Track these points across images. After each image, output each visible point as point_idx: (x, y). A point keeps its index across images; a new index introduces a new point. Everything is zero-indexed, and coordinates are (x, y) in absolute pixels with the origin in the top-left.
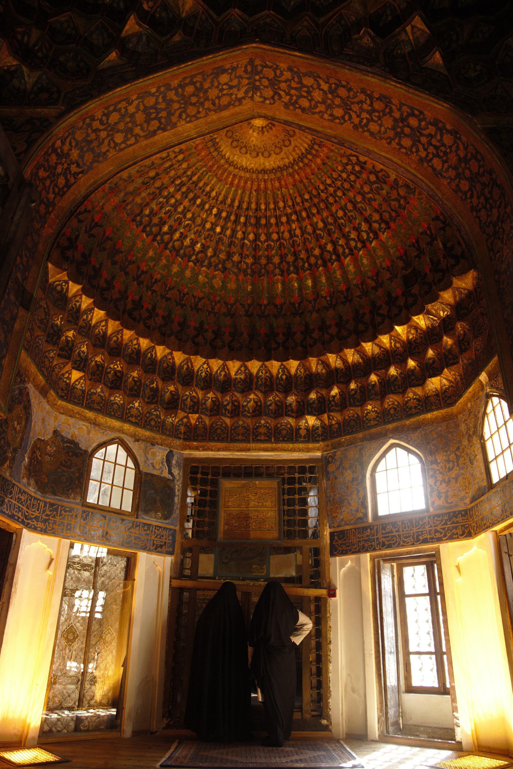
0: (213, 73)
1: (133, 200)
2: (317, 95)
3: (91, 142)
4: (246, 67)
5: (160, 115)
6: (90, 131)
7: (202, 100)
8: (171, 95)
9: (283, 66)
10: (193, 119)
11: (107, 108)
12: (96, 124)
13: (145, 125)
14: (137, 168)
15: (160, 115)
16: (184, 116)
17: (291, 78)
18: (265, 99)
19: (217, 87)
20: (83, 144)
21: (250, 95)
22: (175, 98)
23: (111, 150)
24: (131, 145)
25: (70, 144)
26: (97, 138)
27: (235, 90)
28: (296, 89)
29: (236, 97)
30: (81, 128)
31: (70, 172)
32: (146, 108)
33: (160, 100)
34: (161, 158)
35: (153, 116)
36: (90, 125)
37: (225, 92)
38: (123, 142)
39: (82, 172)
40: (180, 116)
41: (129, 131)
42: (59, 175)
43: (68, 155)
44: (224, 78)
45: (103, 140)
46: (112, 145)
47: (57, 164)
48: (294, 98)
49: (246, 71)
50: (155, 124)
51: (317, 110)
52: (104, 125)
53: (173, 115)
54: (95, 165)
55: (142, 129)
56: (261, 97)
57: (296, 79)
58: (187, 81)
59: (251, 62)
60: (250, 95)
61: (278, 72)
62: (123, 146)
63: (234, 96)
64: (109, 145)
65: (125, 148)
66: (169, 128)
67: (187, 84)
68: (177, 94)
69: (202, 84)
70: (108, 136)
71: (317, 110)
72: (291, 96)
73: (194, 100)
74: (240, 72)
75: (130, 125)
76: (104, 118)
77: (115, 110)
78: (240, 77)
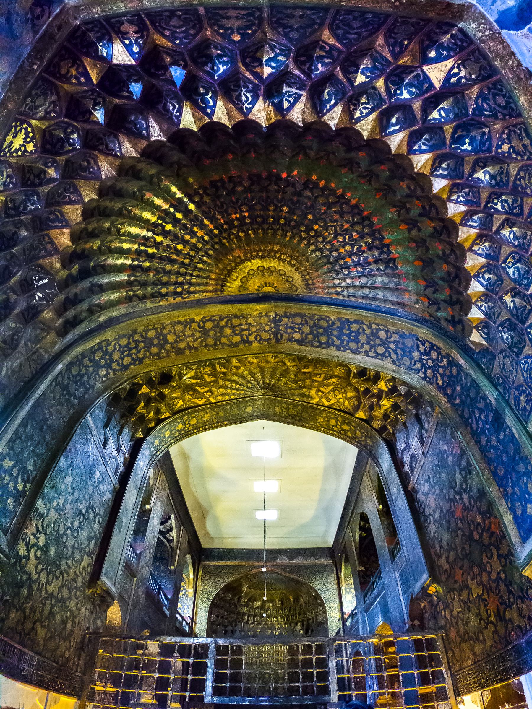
0: (306, 343)
1: (390, 281)
2: (228, 331)
3: (402, 349)
4: (282, 338)
5: (348, 332)
6: (400, 357)
7: (315, 328)
8: (337, 342)
9: (255, 344)
10: (324, 317)
11: (382, 360)
12: (394, 356)
13: (361, 331)
14: (377, 302)
15: (348, 332)
16: (330, 322)
17: (250, 337)
18: (266, 315)
19: (303, 333)
20: (407, 353)
21: (278, 317)
22: (335, 339)
23: (391, 331)
24: (377, 324)
25: (415, 364)
26: (397, 347)
27: (290, 325)
28: (244, 330)
29: (289, 319)
30: (403, 364)
31: (425, 350)
32: (357, 341)
33: (345, 342)
34: (356, 297)
35: (353, 334)
36: (398, 360)
37: (297, 326)
38: (382, 330)
39: (418, 339)
40: (333, 323)
41: (375, 334)
42: (433, 362)
43: (420, 361)
44: (297, 336)
45: (394, 342)
46: (389, 334)
47: (430, 367)
48: (244, 323)
49: (282, 336)
50: (354, 327)
51: (225, 320)
52: (389, 352)
53: (338, 327)
54: (407, 333)
55: (364, 330)
56: (270, 316)
57: (245, 337)
58: (324, 346)
59: (278, 341)
60: (278, 317)
61: (258, 338)
62: (382, 327)
63: (290, 320)
64: (391, 336)
65: (382, 325)
66: (344, 319)
67: (324, 343)
68: (333, 341)
69: (314, 339)
70: (390, 342)
71: (225, 320)
72: (246, 324)
73: (321, 331)
74: (286, 336)
75: (372, 338)
76: (387, 355)
77: (378, 354)
78: (286, 333)
